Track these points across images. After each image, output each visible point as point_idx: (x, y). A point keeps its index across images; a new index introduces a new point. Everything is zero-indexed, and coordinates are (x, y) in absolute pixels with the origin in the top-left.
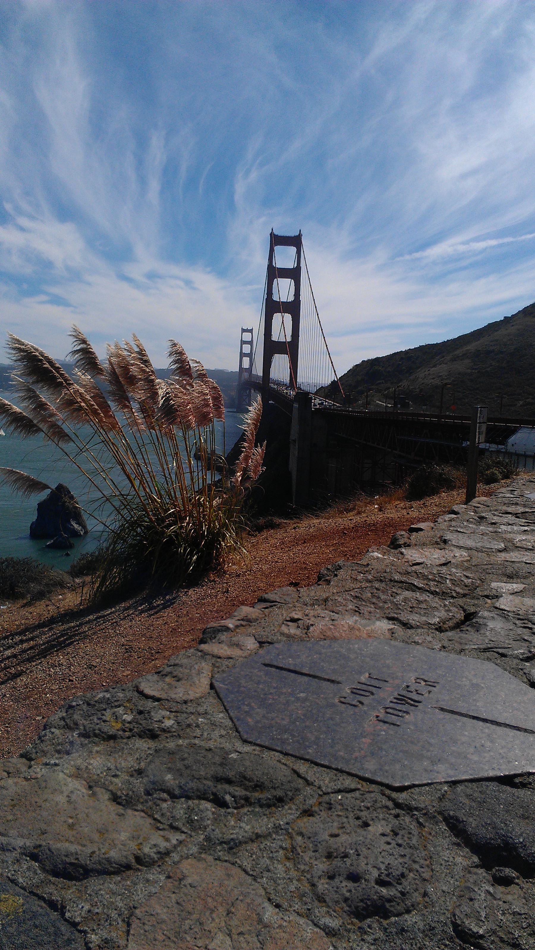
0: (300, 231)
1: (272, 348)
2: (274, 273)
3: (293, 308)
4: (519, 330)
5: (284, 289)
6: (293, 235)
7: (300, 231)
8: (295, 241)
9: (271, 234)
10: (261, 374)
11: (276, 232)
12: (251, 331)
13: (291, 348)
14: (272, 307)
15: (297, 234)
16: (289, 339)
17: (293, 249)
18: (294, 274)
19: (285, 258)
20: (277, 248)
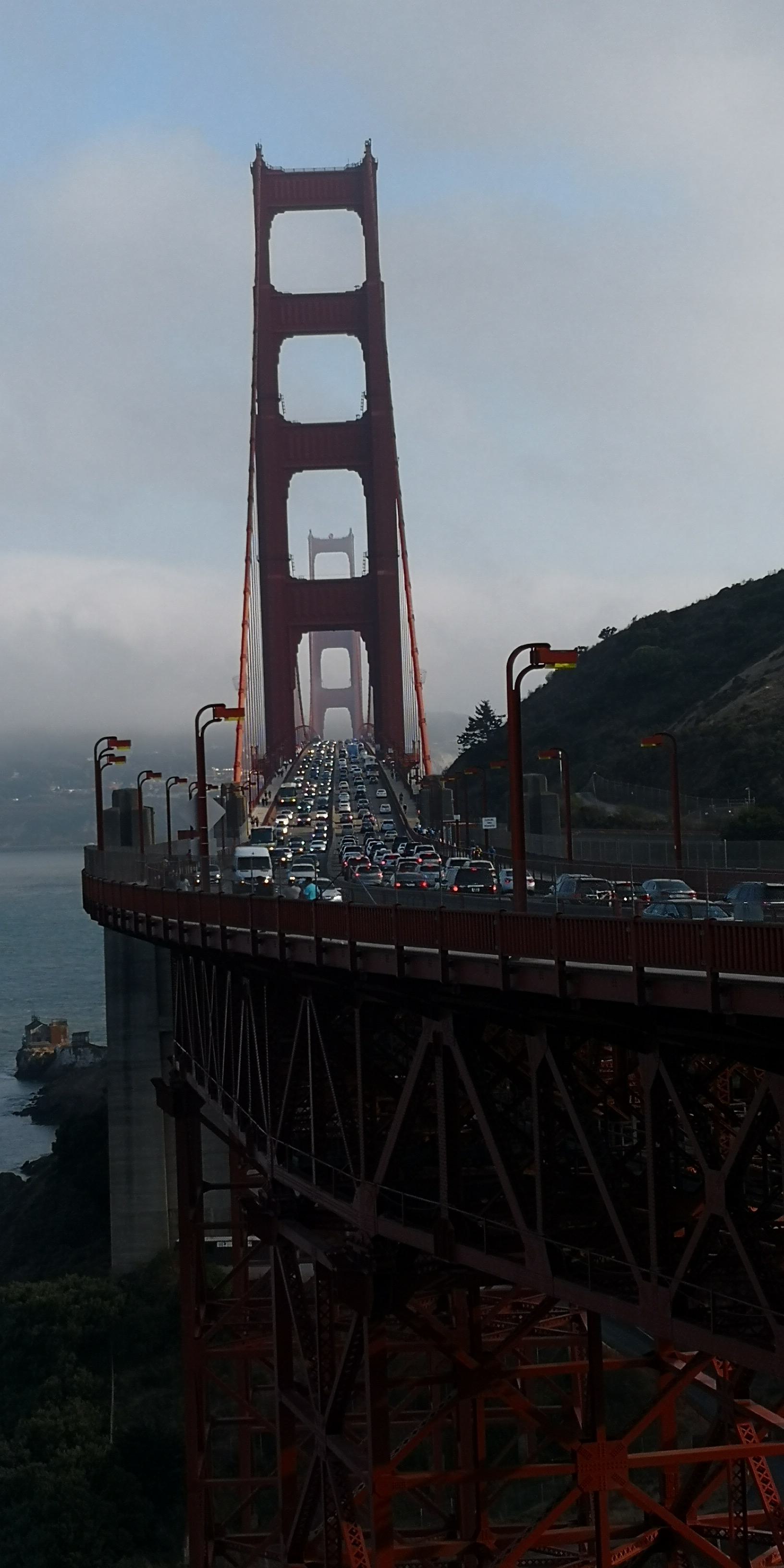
0: (368, 146)
1: (290, 608)
2: (280, 316)
3: (366, 446)
5: (322, 380)
6: (339, 164)
7: (368, 146)
8: (352, 189)
9: (253, 170)
11: (273, 161)
12: (345, 545)
13: (369, 607)
15: (357, 158)
17: (348, 220)
18: (359, 313)
19: (316, 252)
20: (284, 223)
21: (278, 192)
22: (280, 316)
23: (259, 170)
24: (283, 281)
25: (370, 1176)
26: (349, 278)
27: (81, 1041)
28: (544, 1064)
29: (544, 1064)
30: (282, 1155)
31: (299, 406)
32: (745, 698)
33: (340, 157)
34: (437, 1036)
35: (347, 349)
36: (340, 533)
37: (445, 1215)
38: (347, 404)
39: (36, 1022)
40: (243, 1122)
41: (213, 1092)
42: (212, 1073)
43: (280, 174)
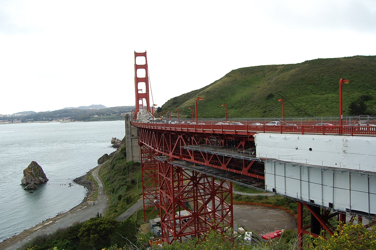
2: (137, 67)
3: (146, 80)
4: (223, 82)
5: (141, 73)
6: (143, 52)
8: (144, 54)
10: (146, 105)
11: (136, 52)
12: (141, 90)
13: (146, 96)
14: (138, 80)
15: (145, 52)
16: (144, 91)
17: (144, 57)
18: (145, 67)
19: (141, 61)
20: (137, 57)
21: (137, 55)
22: (137, 67)
23: (135, 52)
24: (137, 64)
25: (172, 151)
26: (144, 63)
27: (118, 140)
28: (194, 139)
29: (194, 139)
30: (159, 150)
31: (139, 76)
32: (186, 105)
33: (144, 52)
34: (180, 137)
35: (144, 70)
36: (141, 89)
37: (181, 155)
38: (144, 76)
39: (113, 138)
40: (153, 146)
41: (147, 144)
42: (147, 142)
43: (137, 53)
